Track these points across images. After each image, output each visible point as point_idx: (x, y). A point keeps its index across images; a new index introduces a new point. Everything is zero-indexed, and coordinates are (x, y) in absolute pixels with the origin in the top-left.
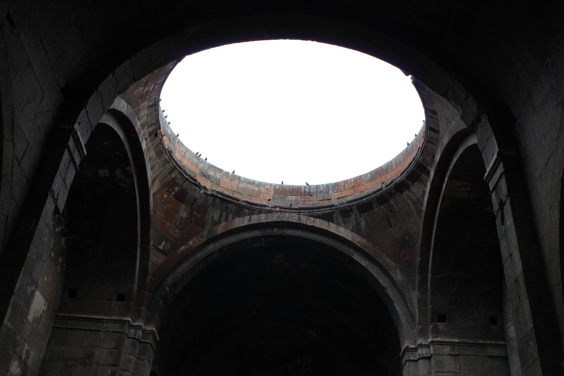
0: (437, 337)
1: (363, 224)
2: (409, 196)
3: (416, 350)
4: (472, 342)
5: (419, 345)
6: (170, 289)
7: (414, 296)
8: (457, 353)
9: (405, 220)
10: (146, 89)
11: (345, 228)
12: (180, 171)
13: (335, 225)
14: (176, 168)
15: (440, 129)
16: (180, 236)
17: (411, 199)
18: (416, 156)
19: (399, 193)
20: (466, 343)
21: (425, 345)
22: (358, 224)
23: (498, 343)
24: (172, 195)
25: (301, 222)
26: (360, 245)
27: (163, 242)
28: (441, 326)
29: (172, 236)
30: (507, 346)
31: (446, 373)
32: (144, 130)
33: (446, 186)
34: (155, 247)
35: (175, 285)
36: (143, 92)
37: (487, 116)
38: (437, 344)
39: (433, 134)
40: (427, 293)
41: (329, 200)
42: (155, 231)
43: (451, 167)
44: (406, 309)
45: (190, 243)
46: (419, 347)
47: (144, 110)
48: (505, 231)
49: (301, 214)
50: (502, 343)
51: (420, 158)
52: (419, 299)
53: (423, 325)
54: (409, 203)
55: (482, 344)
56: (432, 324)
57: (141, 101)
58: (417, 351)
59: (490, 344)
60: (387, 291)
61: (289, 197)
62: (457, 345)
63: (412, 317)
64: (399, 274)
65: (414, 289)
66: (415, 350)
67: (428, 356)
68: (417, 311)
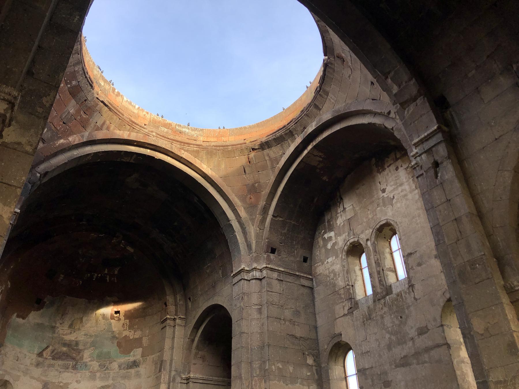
1: (223, 166)
2: (268, 155)
3: (249, 272)
4: (292, 272)
5: (255, 268)
6: (40, 177)
7: (252, 230)
9: (259, 172)
12: (84, 67)
14: (82, 62)
16: (62, 129)
17: (270, 157)
18: (288, 124)
20: (288, 273)
21: (258, 269)
23: (308, 276)
25: (173, 151)
28: (272, 256)
30: (314, 280)
31: (274, 293)
35: (46, 173)
37: (426, 99)
38: (269, 270)
39: (315, 110)
41: (195, 140)
44: (244, 239)
45: (70, 139)
46: (254, 270)
49: (173, 144)
50: (311, 277)
53: (257, 253)
55: (298, 275)
56: (267, 253)
58: (250, 273)
60: (231, 222)
61: (162, 127)
63: (249, 246)
64: (243, 211)
65: (253, 225)
66: (248, 272)
68: (254, 242)
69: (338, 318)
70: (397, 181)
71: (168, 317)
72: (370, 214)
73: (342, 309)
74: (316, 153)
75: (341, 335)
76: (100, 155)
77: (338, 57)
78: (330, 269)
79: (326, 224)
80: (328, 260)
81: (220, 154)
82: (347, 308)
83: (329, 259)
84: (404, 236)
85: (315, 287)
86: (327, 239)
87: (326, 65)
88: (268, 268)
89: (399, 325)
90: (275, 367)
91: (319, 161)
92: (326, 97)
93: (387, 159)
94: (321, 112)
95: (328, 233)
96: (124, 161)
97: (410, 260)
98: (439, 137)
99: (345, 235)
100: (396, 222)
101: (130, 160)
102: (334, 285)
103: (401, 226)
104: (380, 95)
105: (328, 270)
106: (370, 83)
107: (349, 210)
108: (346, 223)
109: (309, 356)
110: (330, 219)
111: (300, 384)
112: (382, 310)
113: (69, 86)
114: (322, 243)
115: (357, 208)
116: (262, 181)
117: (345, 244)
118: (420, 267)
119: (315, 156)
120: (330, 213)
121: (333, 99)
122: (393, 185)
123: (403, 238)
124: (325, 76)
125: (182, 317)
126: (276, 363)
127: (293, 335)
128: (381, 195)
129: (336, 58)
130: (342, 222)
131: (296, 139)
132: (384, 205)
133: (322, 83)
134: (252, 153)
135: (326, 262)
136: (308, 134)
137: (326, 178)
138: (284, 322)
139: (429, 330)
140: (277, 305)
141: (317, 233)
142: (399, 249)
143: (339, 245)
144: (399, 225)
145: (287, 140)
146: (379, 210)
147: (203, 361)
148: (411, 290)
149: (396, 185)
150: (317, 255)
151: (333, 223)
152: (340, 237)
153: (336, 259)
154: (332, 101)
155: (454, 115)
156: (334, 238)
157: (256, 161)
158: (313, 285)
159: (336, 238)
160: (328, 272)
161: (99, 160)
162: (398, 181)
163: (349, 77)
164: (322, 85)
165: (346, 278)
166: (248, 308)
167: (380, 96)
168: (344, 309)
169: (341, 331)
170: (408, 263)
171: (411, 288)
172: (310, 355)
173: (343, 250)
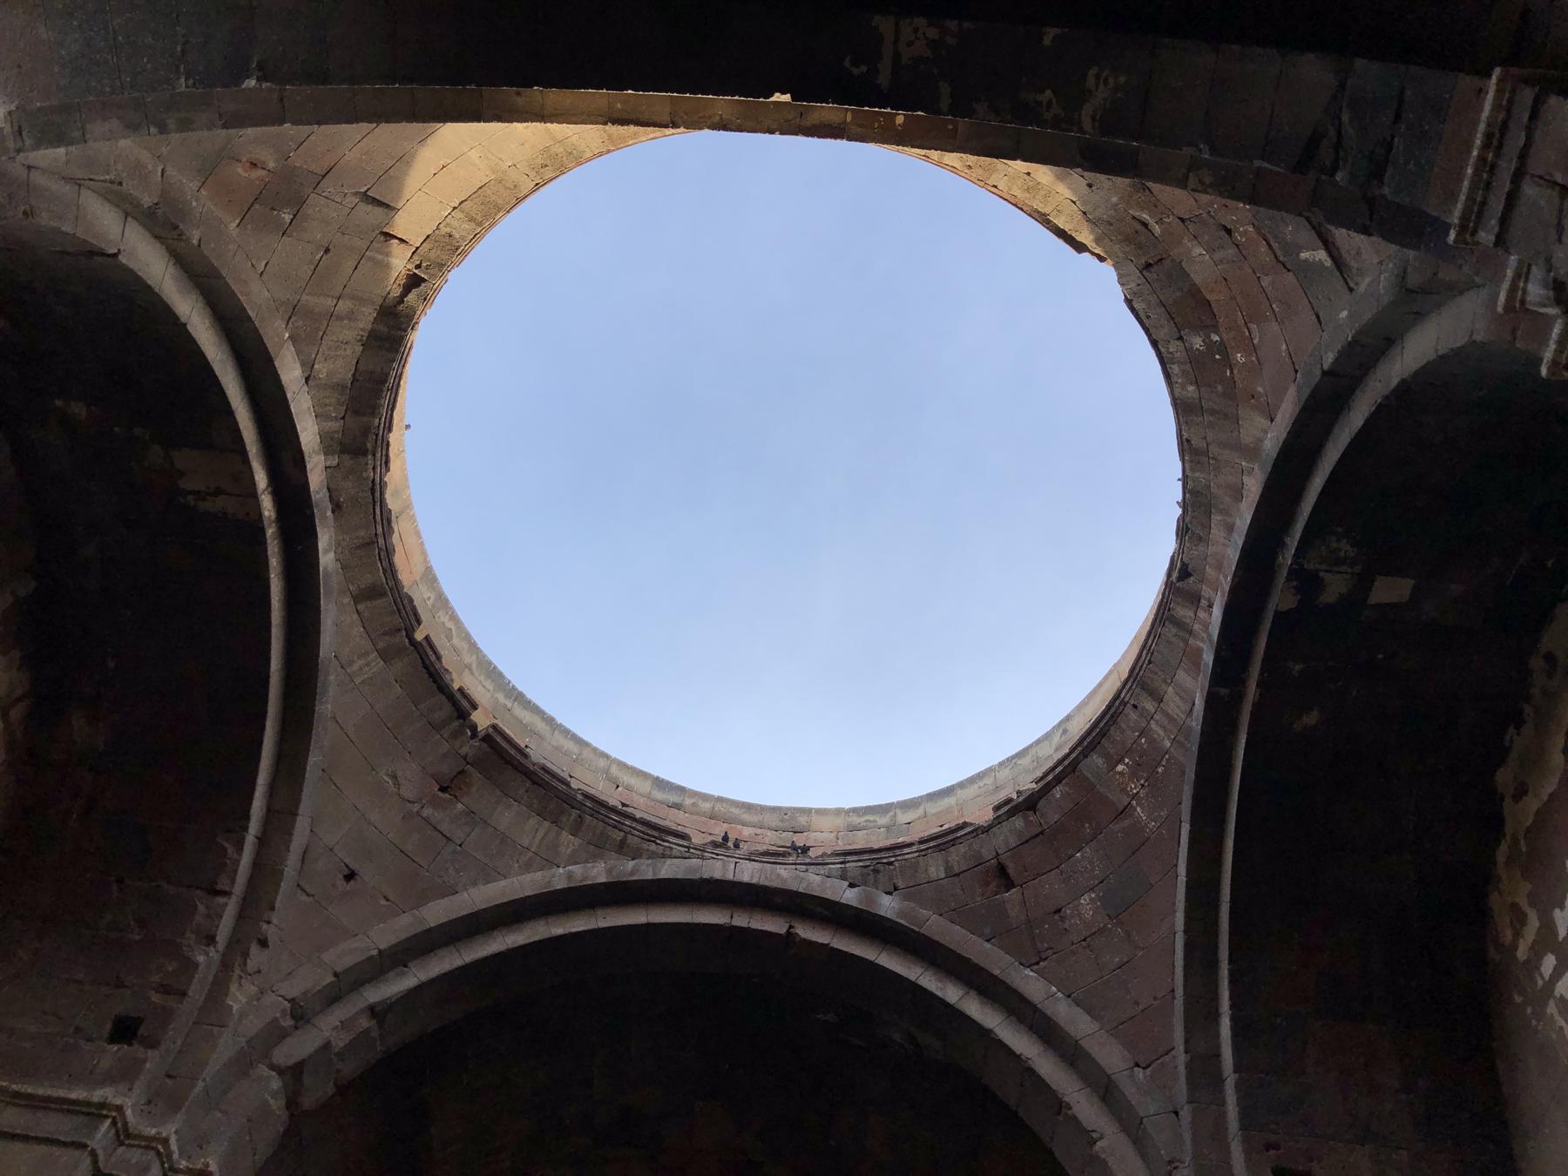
2: (351, 316)
9: (327, 251)
10: (1133, 788)
15: (355, 616)
17: (340, 318)
24: (1221, 338)
27: (1306, 261)
29: (1264, 242)
32: (1201, 645)
33: (253, 495)
34: (1345, 280)
36: (1143, 785)
39: (367, 580)
42: (1321, 314)
43: (274, 562)
47: (1170, 711)
51: (374, 468)
57: (1159, 764)
76: (1048, 93)
77: (462, 772)
87: (460, 706)
92: (381, 645)
94: (347, 600)
96: (920, 21)
101: (897, 33)
104: (313, 896)
106: (354, 866)
113: (1216, 338)
119: (218, 492)
121: (361, 669)
124: (435, 686)
131: (325, 454)
133: (423, 663)
134: (411, 266)
145: (343, 418)
154: (361, 662)
157: (372, 259)
161: (1050, 35)
163: (394, 777)
164: (422, 658)
167: (308, 895)
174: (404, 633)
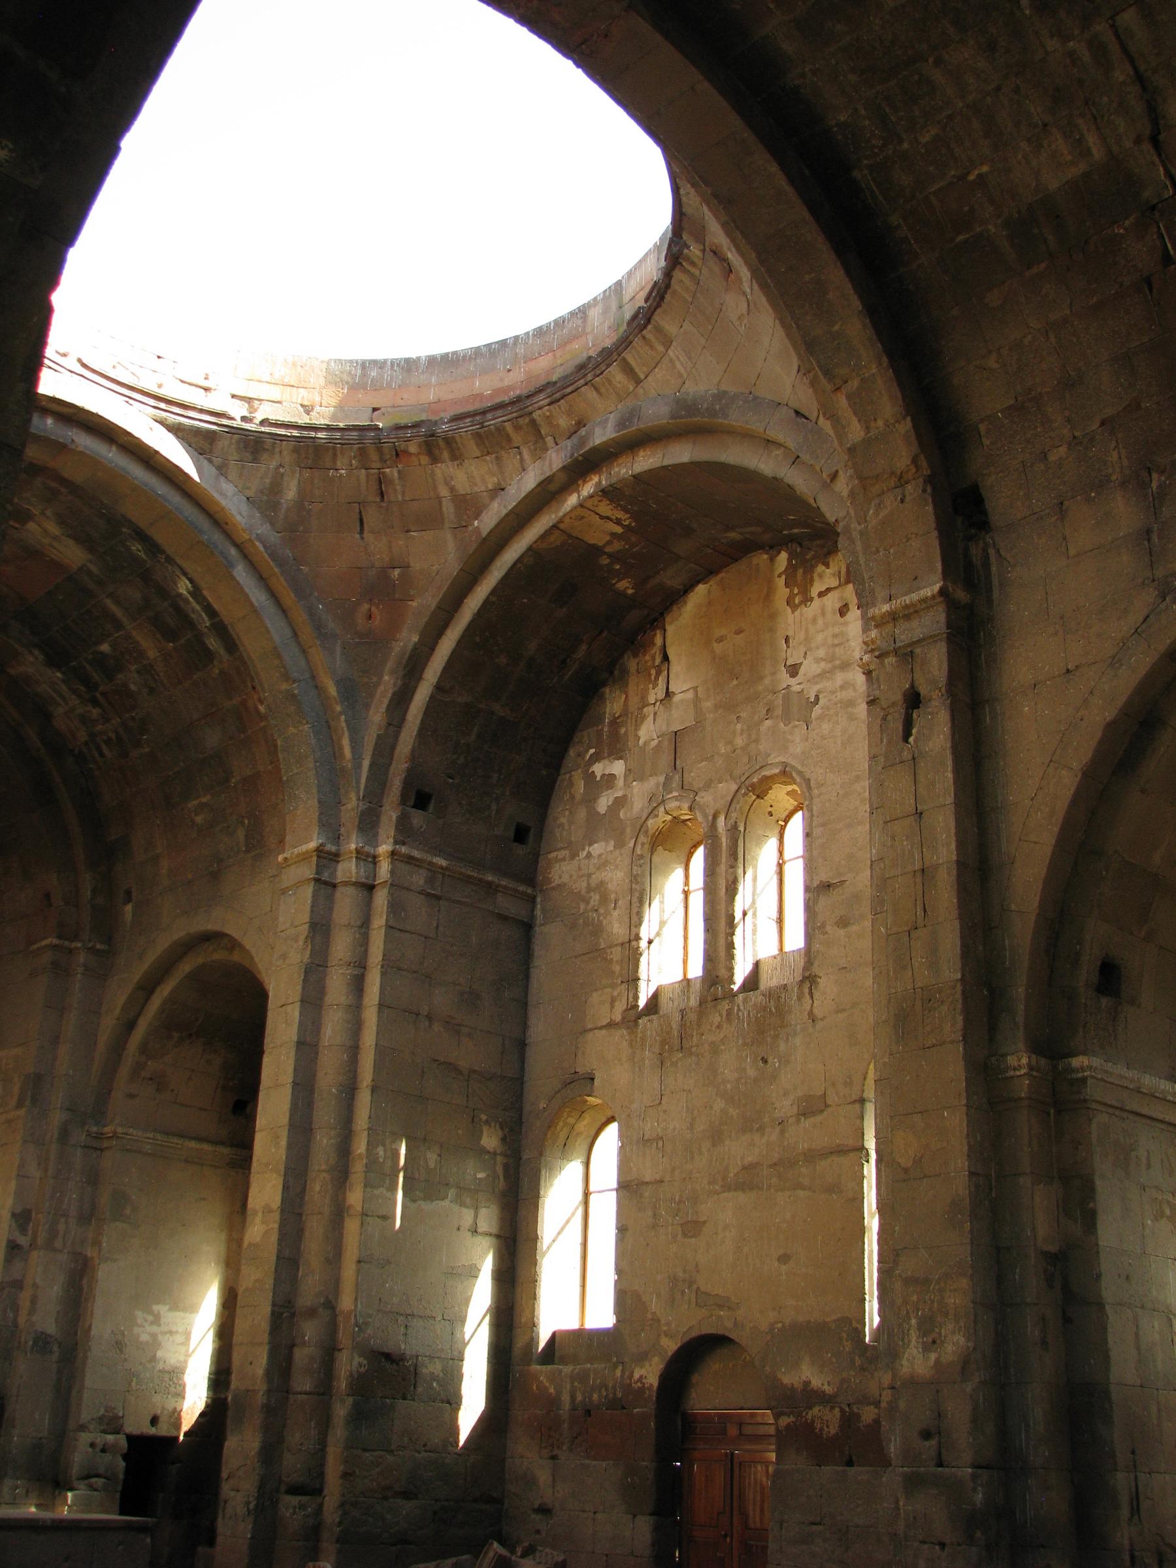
0: (404, 844)
1: (290, 493)
8: (437, 892)
11: (236, 487)
13: (214, 471)
15: (649, 378)
17: (452, 489)
19: (425, 460)
21: (368, 855)
22: (275, 488)
26: (265, 547)
28: (418, 819)
30: (539, 900)
31: (407, 935)
40: (400, 727)
48: (914, 758)
50: (529, 891)
52: (379, 736)
54: (442, 495)
55: (489, 884)
58: (338, 862)
59: (506, 887)
62: (440, 873)
67: (370, 882)
69: (591, 1030)
70: (837, 650)
71: (55, 941)
72: (741, 734)
73: (608, 1005)
74: (605, 508)
75: (593, 1079)
77: (715, 253)
78: (594, 876)
79: (606, 729)
80: (591, 849)
81: (285, 453)
82: (620, 1006)
83: (596, 845)
84: (822, 828)
85: (538, 922)
86: (598, 779)
88: (400, 855)
89: (756, 1080)
90: (385, 1151)
91: (613, 535)
92: (661, 348)
93: (820, 568)
95: (606, 762)
97: (823, 902)
98: (935, 621)
99: (656, 781)
100: (809, 779)
102: (597, 930)
103: (820, 794)
105: (585, 879)
107: (682, 701)
108: (666, 743)
109: (490, 1126)
110: (619, 717)
111: (452, 1202)
112: (718, 1031)
114: (582, 791)
115: (708, 704)
116: (416, 565)
117: (650, 810)
118: (846, 930)
119: (602, 517)
120: (624, 696)
122: (822, 658)
123: (817, 832)
124: (669, 291)
125: (98, 946)
126: (388, 1141)
127: (451, 1064)
128: (784, 679)
129: (709, 255)
130: (655, 737)
131: (547, 450)
132: (787, 717)
135: (585, 853)
136: (587, 448)
137: (628, 585)
138: (427, 1024)
139: (826, 1106)
140: (415, 972)
141: (572, 752)
142: (802, 857)
143: (632, 808)
144: (816, 792)
145: (518, 448)
146: (769, 729)
147: (158, 1090)
148: (806, 991)
149: (830, 662)
150: (562, 825)
151: (626, 732)
152: (640, 784)
153: (617, 852)
155: (993, 559)
156: (620, 782)
157: (403, 494)
158: (532, 917)
159: (627, 785)
160: (584, 884)
162: (839, 651)
165: (635, 915)
166: (321, 969)
168: (612, 1007)
169: (595, 1070)
170: (817, 910)
171: (807, 984)
172: (493, 1124)
173: (641, 827)
174: (644, 332)
